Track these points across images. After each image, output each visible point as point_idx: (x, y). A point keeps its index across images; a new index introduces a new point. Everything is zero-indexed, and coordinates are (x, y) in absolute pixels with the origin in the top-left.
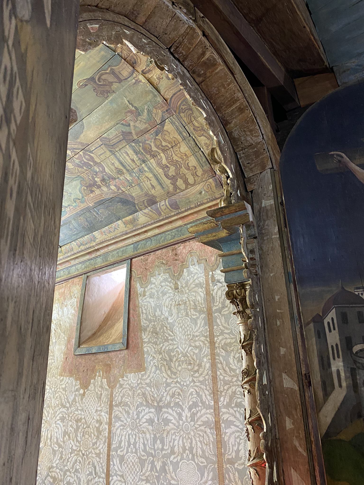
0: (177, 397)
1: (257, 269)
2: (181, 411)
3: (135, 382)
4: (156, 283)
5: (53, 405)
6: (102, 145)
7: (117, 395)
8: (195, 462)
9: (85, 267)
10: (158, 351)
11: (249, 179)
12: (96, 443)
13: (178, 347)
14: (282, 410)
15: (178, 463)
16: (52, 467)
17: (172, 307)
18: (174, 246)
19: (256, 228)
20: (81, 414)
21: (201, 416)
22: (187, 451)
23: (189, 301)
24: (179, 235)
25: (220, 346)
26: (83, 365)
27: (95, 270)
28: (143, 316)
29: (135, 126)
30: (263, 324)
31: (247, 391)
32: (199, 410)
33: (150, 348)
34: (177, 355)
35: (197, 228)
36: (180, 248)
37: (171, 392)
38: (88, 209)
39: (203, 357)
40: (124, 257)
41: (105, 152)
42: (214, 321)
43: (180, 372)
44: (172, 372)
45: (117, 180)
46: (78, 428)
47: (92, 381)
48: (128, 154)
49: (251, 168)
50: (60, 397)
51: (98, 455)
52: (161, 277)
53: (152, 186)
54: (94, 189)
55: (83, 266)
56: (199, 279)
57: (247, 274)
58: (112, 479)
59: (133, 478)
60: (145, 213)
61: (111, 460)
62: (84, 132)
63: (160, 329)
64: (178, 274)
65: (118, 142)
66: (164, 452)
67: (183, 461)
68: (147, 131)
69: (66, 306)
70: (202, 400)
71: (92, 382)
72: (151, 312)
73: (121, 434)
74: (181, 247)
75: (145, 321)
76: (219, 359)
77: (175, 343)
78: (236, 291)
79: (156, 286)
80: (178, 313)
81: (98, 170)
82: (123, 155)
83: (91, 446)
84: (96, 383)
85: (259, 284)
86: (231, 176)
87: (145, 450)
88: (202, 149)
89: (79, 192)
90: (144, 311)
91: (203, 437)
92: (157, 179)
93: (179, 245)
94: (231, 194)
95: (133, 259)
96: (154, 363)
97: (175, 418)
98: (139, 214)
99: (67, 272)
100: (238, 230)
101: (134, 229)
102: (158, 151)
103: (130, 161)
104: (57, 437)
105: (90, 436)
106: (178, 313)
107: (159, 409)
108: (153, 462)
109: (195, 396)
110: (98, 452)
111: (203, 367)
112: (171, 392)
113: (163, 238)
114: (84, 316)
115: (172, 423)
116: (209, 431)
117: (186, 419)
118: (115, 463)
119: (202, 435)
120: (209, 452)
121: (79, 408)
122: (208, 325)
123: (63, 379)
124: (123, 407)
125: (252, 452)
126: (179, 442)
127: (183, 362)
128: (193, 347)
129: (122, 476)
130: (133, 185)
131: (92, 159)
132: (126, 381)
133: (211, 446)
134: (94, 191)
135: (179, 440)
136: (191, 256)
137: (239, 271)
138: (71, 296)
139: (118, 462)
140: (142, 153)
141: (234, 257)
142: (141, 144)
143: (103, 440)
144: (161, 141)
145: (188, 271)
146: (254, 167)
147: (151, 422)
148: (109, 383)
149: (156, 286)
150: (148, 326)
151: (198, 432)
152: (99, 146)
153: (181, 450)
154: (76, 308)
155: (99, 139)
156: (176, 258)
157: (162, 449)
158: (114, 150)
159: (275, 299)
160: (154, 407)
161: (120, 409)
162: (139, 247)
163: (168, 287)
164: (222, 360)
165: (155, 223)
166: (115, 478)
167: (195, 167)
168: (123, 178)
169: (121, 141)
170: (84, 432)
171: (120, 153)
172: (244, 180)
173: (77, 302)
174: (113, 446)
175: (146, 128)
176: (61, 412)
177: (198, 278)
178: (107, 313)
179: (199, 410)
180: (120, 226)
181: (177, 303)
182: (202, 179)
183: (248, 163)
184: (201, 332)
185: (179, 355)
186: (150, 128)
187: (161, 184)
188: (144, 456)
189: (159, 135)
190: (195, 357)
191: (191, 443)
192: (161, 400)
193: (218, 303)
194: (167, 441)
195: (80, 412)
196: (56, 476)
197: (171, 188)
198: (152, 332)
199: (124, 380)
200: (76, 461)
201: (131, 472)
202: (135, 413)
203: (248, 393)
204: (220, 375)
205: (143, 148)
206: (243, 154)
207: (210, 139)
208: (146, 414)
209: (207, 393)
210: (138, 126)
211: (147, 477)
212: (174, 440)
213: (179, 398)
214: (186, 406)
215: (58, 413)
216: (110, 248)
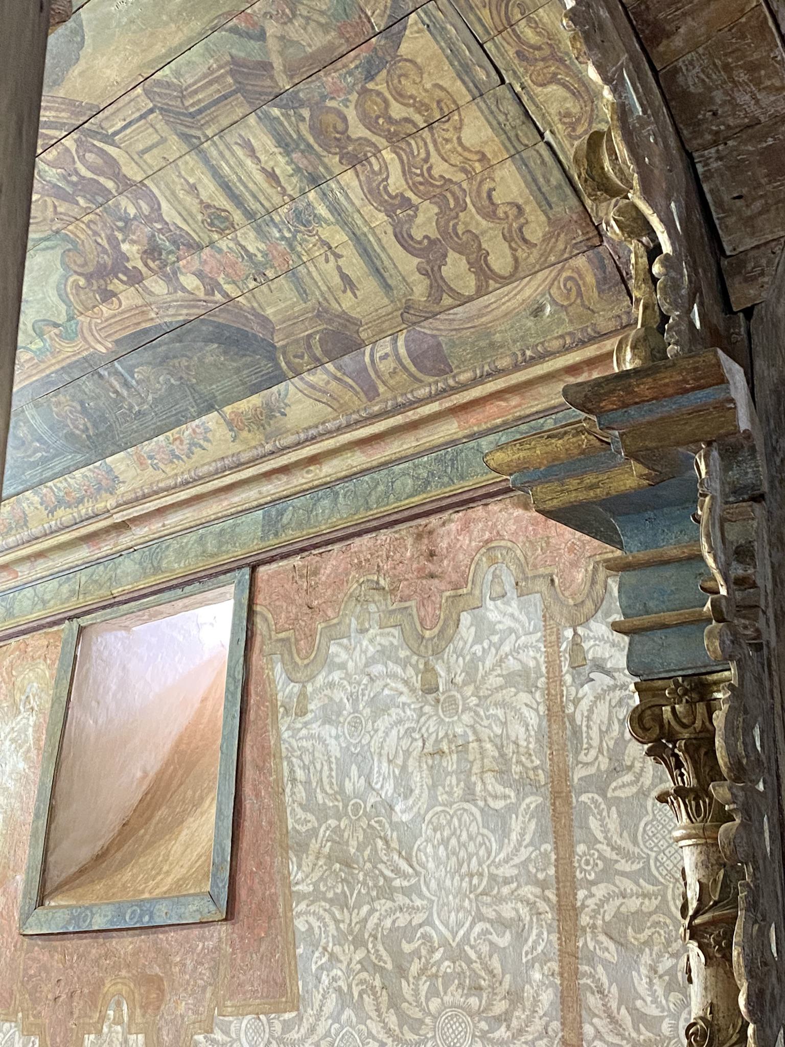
1: (761, 624)
4: (350, 665)
6: (151, 111)
9: (73, 593)
10: (351, 932)
11: (740, 261)
13: (428, 922)
17: (411, 762)
18: (422, 521)
19: (760, 459)
23: (479, 740)
24: (446, 479)
25: (599, 922)
27: (111, 605)
28: (293, 793)
29: (282, 38)
33: (320, 918)
34: (424, 952)
35: (521, 454)
36: (450, 530)
38: (90, 366)
39: (530, 965)
40: (224, 558)
41: (163, 140)
42: (575, 824)
43: (435, 1018)
44: (403, 1019)
45: (207, 251)
48: (254, 153)
49: (751, 218)
52: (371, 641)
53: (344, 277)
54: (116, 285)
55: (65, 589)
56: (522, 656)
57: (722, 643)
60: (313, 387)
62: (82, 61)
63: (360, 848)
64: (436, 630)
65: (216, 102)
68: (329, 61)
72: (325, 780)
74: (453, 526)
75: (301, 814)
76: (591, 976)
77: (418, 903)
78: (673, 709)
79: (348, 676)
81: (132, 211)
82: (233, 154)
85: (767, 683)
86: (667, 248)
88: (547, 135)
89: (55, 299)
90: (300, 774)
92: (366, 253)
93: (445, 516)
94: (665, 318)
95: (262, 570)
96: (334, 979)
98: (290, 389)
100: (689, 464)
101: (269, 447)
102: (374, 139)
103: (259, 177)
111: (528, 1004)
113: (381, 488)
114: (62, 784)
122: (551, 837)
127: (447, 980)
128: (491, 921)
130: (270, 274)
131: (112, 167)
134: (114, 295)
136: (493, 561)
137: (685, 629)
138: (15, 704)
140: (309, 146)
141: (669, 572)
142: (306, 113)
144: (385, 101)
145: (479, 622)
146: (760, 213)
149: (348, 676)
150: (314, 832)
152: (142, 117)
154: (33, 754)
155: (139, 90)
156: (431, 567)
158: (198, 133)
163: (397, 683)
164: (605, 980)
165: (350, 426)
167: (519, 207)
168: (231, 245)
169: (225, 97)
171: (222, 147)
172: (718, 263)
173: (37, 728)
175: (330, 47)
177: (516, 650)
178: (152, 774)
180: (212, 435)
181: (429, 748)
182: (545, 255)
183: (739, 197)
184: (525, 863)
185: (432, 951)
186: (344, 49)
187: (378, 272)
189: (378, 78)
190: (496, 963)
193: (593, 753)
197: (420, 289)
198: (329, 857)
199: (214, 1041)
204: (595, 1038)
205: (312, 128)
206: (720, 158)
207: (587, 95)
210: (294, 36)
216: (174, 520)
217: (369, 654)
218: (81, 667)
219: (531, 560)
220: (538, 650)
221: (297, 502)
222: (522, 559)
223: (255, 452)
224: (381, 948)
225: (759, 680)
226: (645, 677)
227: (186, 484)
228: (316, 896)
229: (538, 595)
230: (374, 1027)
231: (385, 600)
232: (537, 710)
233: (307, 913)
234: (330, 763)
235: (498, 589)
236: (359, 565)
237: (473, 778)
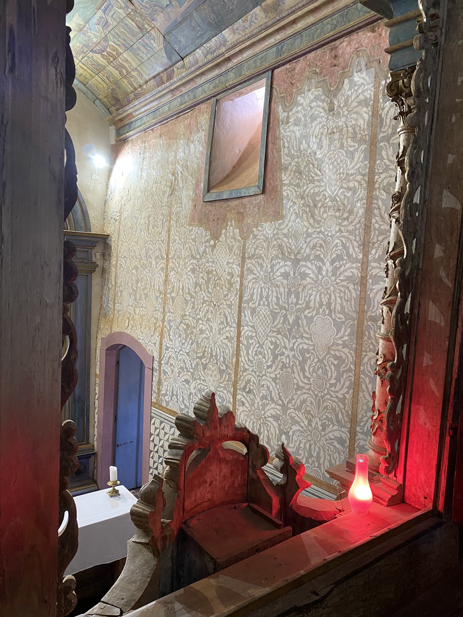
0: (319, 249)
2: (321, 265)
3: (270, 232)
4: (304, 104)
5: (183, 256)
7: (250, 246)
8: (332, 318)
9: (214, 87)
10: (300, 195)
12: (227, 295)
13: (325, 190)
14: (433, 237)
15: (312, 317)
16: (185, 315)
17: (323, 137)
18: (333, 43)
20: (212, 266)
21: (345, 271)
22: (324, 307)
23: (347, 127)
25: (381, 186)
26: (213, 213)
27: (226, 90)
30: (431, 121)
31: (394, 220)
32: (343, 264)
33: (291, 191)
34: (323, 200)
37: (311, 243)
39: (357, 201)
40: (263, 67)
42: (377, 153)
43: (325, 220)
46: (209, 279)
47: (223, 231)
50: (190, 248)
51: (230, 306)
52: (312, 94)
55: (211, 86)
56: (365, 94)
58: (243, 329)
59: (264, 329)
61: (242, 312)
63: (305, 168)
64: (335, 87)
66: (298, 307)
67: (318, 316)
69: (193, 142)
70: (348, 253)
71: (223, 232)
72: (294, 146)
73: (254, 287)
74: (345, 44)
75: (286, 158)
76: (377, 204)
77: (322, 184)
78: (403, 81)
79: (304, 108)
80: (330, 144)
83: (223, 297)
84: (228, 234)
85: (437, 60)
87: (277, 304)
90: (286, 145)
91: (345, 293)
93: (342, 40)
96: (294, 210)
97: (313, 272)
99: (192, 96)
101: (278, 18)
104: (188, 288)
105: (222, 288)
106: (330, 144)
107: (296, 262)
108: (285, 316)
109: (341, 248)
110: (229, 303)
111: (355, 214)
112: (311, 243)
113: (319, 31)
115: (310, 278)
116: (352, 286)
117: (327, 274)
118: (247, 315)
119: (343, 290)
120: (349, 308)
121: (210, 260)
122: (368, 159)
123: (192, 229)
124: (256, 260)
125: (388, 289)
126: (315, 297)
127: (330, 208)
128: (345, 188)
129: (253, 327)
132: (261, 231)
133: (353, 303)
135: (316, 295)
136: (358, 56)
138: (198, 129)
139: (249, 314)
143: (235, 292)
147: (286, 275)
148: (241, 233)
150: (290, 163)
151: (339, 288)
153: (317, 305)
154: (204, 144)
157: (297, 303)
159: (455, 81)
160: (290, 259)
161: (254, 262)
162: (284, 50)
164: (381, 205)
166: (246, 328)
170: (215, 284)
173: (205, 136)
174: (245, 298)
176: (191, 264)
177: (363, 91)
178: (242, 151)
179: (343, 264)
181: (330, 131)
184: (358, 169)
185: (325, 199)
188: (276, 309)
190: (346, 202)
191: (330, 299)
192: (299, 253)
193: (387, 127)
194: (302, 296)
195: (210, 264)
196: (190, 323)
198: (295, 171)
199: (258, 230)
200: (208, 311)
201: (262, 324)
202: (269, 266)
203: (396, 222)
204: (375, 223)
208: (282, 267)
209: (356, 244)
211: (278, 329)
212: (311, 295)
213: (320, 251)
214: (328, 260)
215: (188, 264)
216: (246, 55)
217: (311, 99)
218: (218, 114)
219: (372, 54)
220: (371, 90)
221: (288, 42)
222: (369, 54)
223: (273, 21)
224: (309, 199)
225: (434, 59)
226: (395, 70)
227: (249, 38)
228: (290, 184)
229: (373, 68)
230: (306, 223)
231: (318, 77)
232: (368, 114)
233: (287, 190)
234: (296, 140)
235: (359, 68)
236: (310, 65)
237: (344, 141)
